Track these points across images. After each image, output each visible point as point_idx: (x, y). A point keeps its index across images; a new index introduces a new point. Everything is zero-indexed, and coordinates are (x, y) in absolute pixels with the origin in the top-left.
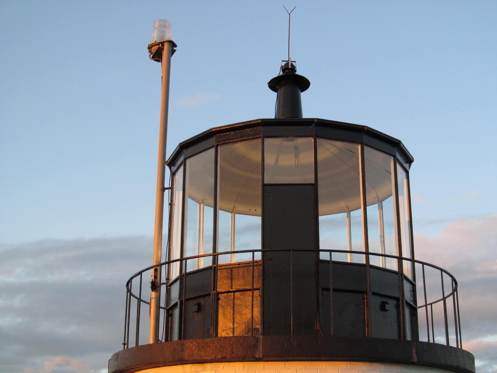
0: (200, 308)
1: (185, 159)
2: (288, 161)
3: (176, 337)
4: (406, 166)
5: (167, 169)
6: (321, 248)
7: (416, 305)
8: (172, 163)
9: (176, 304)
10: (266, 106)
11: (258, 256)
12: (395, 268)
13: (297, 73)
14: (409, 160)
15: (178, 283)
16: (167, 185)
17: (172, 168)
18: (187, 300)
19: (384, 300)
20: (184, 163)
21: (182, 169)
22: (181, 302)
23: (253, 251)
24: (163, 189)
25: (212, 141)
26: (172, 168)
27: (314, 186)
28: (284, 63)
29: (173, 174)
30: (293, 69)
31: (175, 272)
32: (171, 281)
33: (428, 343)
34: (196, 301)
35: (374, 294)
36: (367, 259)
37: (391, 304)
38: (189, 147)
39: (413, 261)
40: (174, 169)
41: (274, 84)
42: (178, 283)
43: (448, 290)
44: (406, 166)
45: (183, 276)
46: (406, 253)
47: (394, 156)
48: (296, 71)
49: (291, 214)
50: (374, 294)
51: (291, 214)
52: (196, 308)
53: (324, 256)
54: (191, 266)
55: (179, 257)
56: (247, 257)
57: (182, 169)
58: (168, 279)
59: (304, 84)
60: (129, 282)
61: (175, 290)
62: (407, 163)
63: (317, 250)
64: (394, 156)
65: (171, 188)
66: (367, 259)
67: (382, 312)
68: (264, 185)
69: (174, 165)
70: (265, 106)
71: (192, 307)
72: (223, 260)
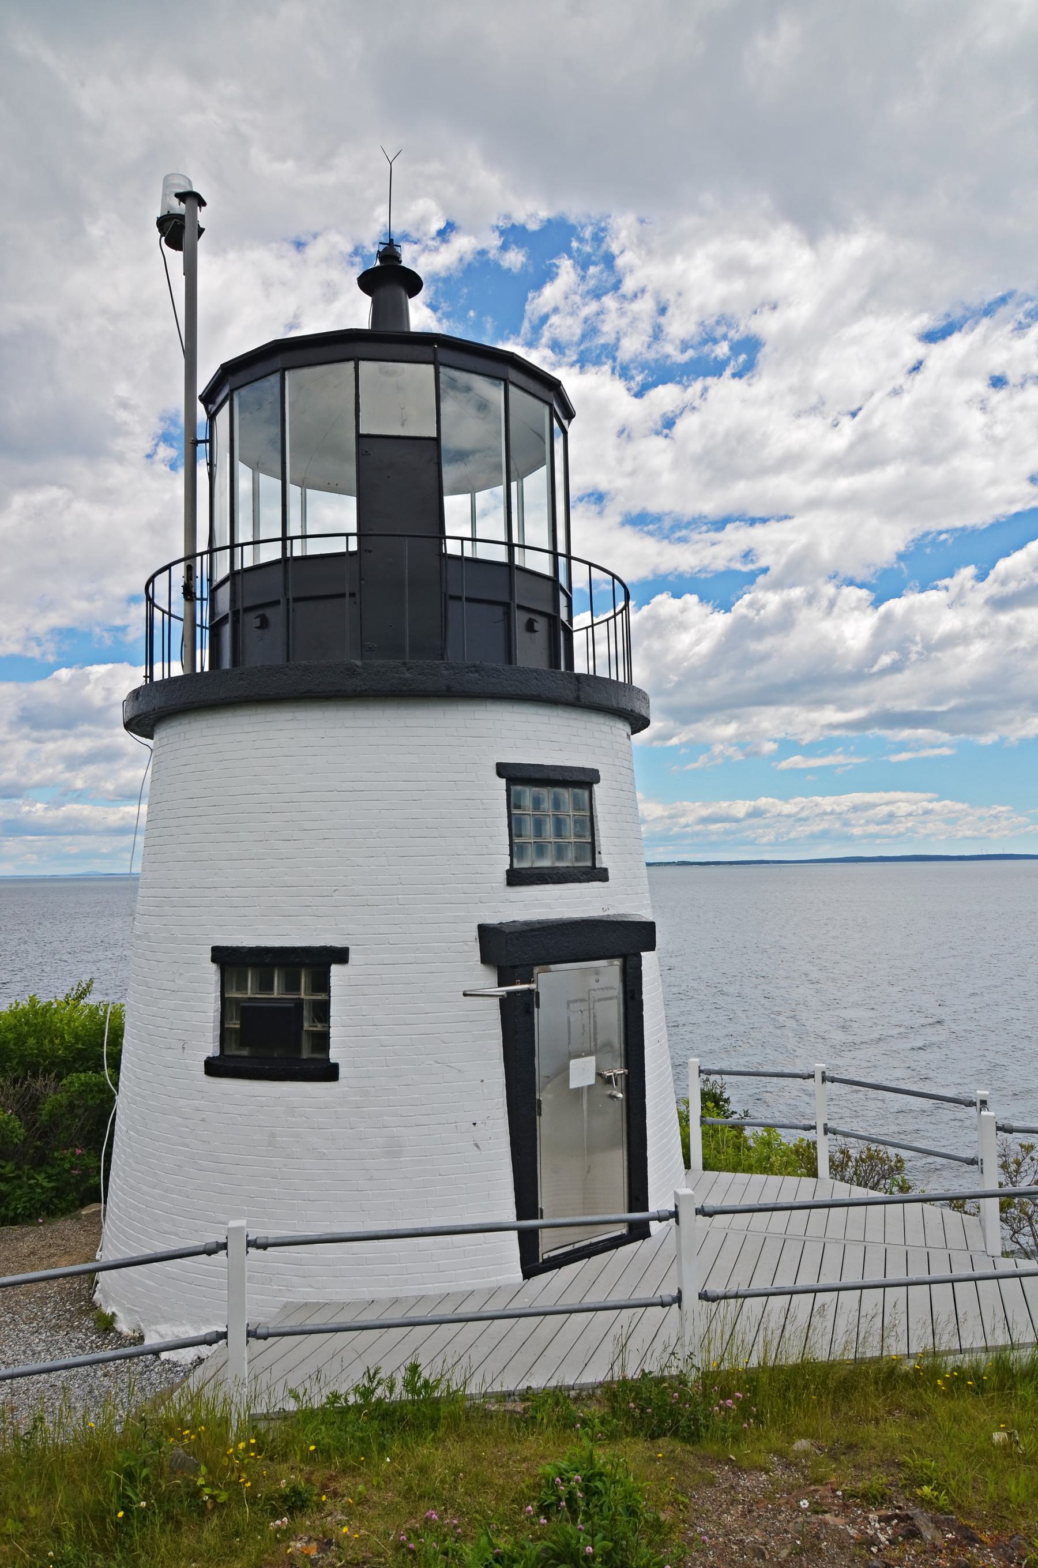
0: (264, 624)
1: (232, 391)
2: (399, 399)
3: (226, 664)
4: (565, 422)
5: (200, 407)
6: (447, 534)
7: (571, 623)
8: (208, 398)
9: (226, 617)
10: (357, 312)
11: (353, 547)
12: (546, 570)
13: (402, 264)
14: (570, 415)
15: (228, 584)
16: (201, 435)
17: (210, 406)
18: (247, 610)
19: (533, 616)
20: (230, 397)
21: (226, 407)
22: (235, 613)
23: (347, 535)
24: (196, 443)
25: (278, 361)
26: (210, 406)
27: (437, 440)
28: (382, 248)
29: (212, 417)
30: (397, 258)
31: (223, 570)
32: (215, 584)
33: (587, 676)
34: (260, 612)
35: (520, 607)
36: (511, 555)
37: (541, 624)
38: (236, 372)
39: (569, 557)
40: (213, 408)
41: (368, 282)
42: (228, 584)
43: (621, 605)
44: (565, 422)
45: (238, 572)
46: (561, 549)
47: (551, 405)
48: (401, 262)
49: (400, 481)
50: (520, 607)
51: (400, 481)
52: (257, 622)
53: (452, 548)
54: (248, 559)
55: (228, 544)
56: (337, 546)
57: (227, 405)
58: (210, 580)
59: (413, 284)
60: (151, 580)
61: (224, 594)
62: (566, 418)
63: (441, 537)
64: (551, 405)
65: (210, 441)
66: (511, 555)
67: (528, 634)
68: (359, 437)
69: (213, 402)
70: (357, 312)
71: (251, 621)
72: (297, 550)
